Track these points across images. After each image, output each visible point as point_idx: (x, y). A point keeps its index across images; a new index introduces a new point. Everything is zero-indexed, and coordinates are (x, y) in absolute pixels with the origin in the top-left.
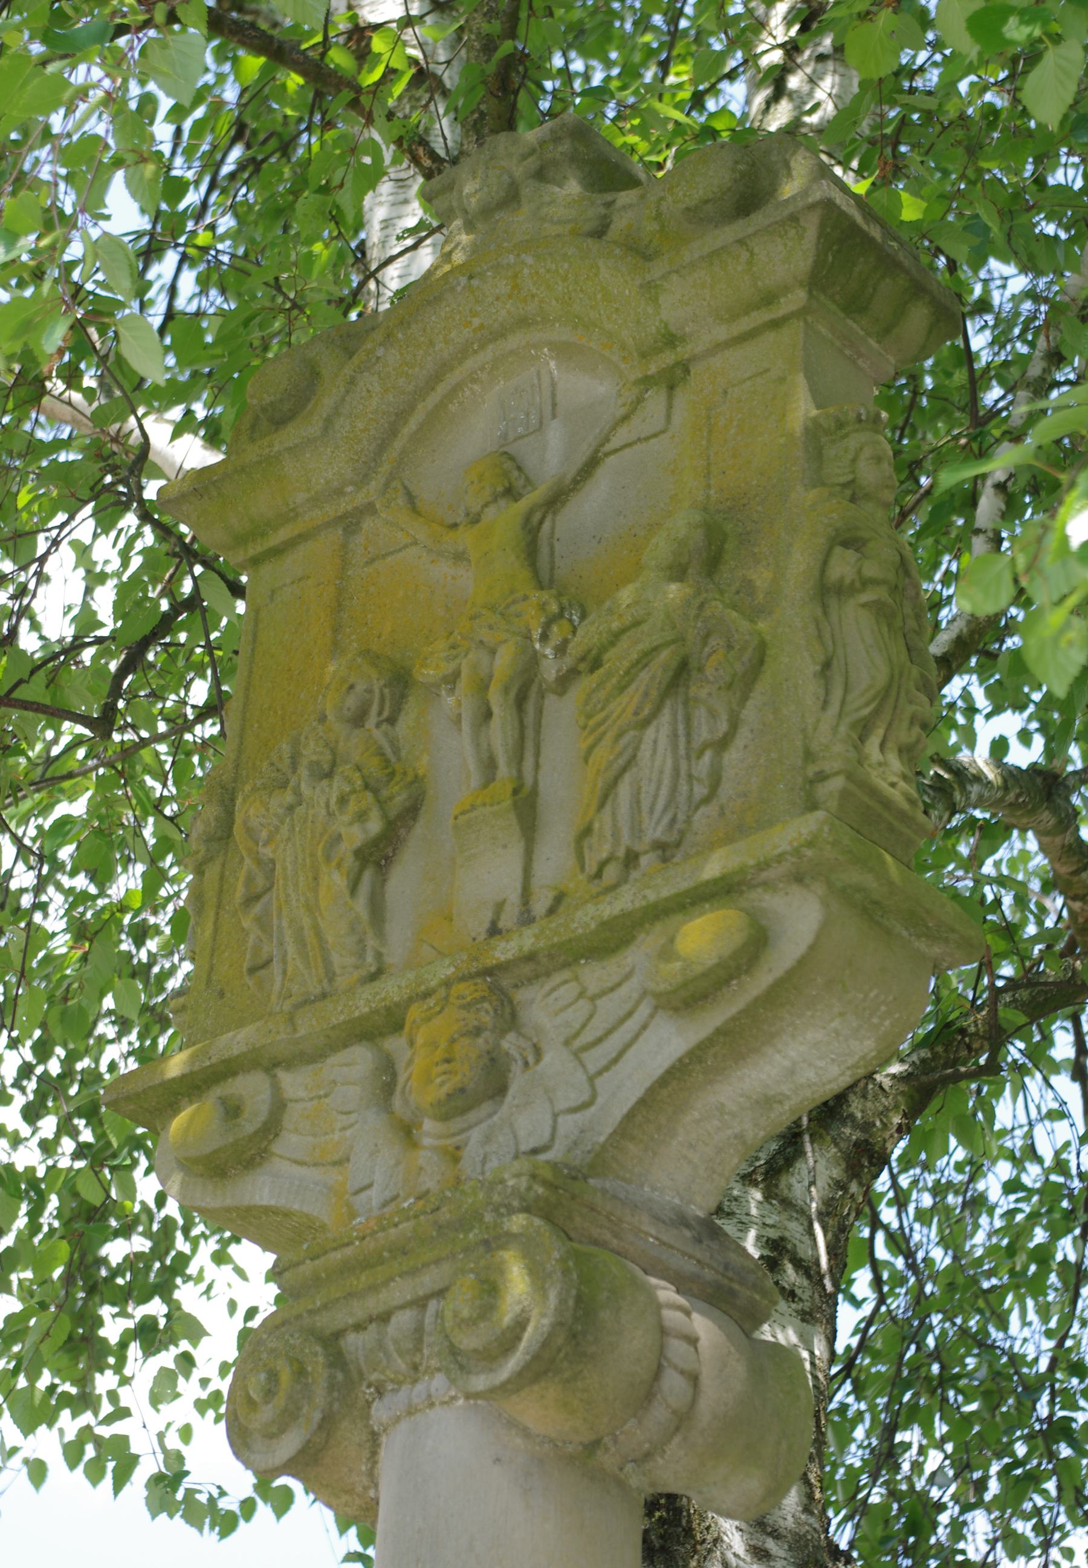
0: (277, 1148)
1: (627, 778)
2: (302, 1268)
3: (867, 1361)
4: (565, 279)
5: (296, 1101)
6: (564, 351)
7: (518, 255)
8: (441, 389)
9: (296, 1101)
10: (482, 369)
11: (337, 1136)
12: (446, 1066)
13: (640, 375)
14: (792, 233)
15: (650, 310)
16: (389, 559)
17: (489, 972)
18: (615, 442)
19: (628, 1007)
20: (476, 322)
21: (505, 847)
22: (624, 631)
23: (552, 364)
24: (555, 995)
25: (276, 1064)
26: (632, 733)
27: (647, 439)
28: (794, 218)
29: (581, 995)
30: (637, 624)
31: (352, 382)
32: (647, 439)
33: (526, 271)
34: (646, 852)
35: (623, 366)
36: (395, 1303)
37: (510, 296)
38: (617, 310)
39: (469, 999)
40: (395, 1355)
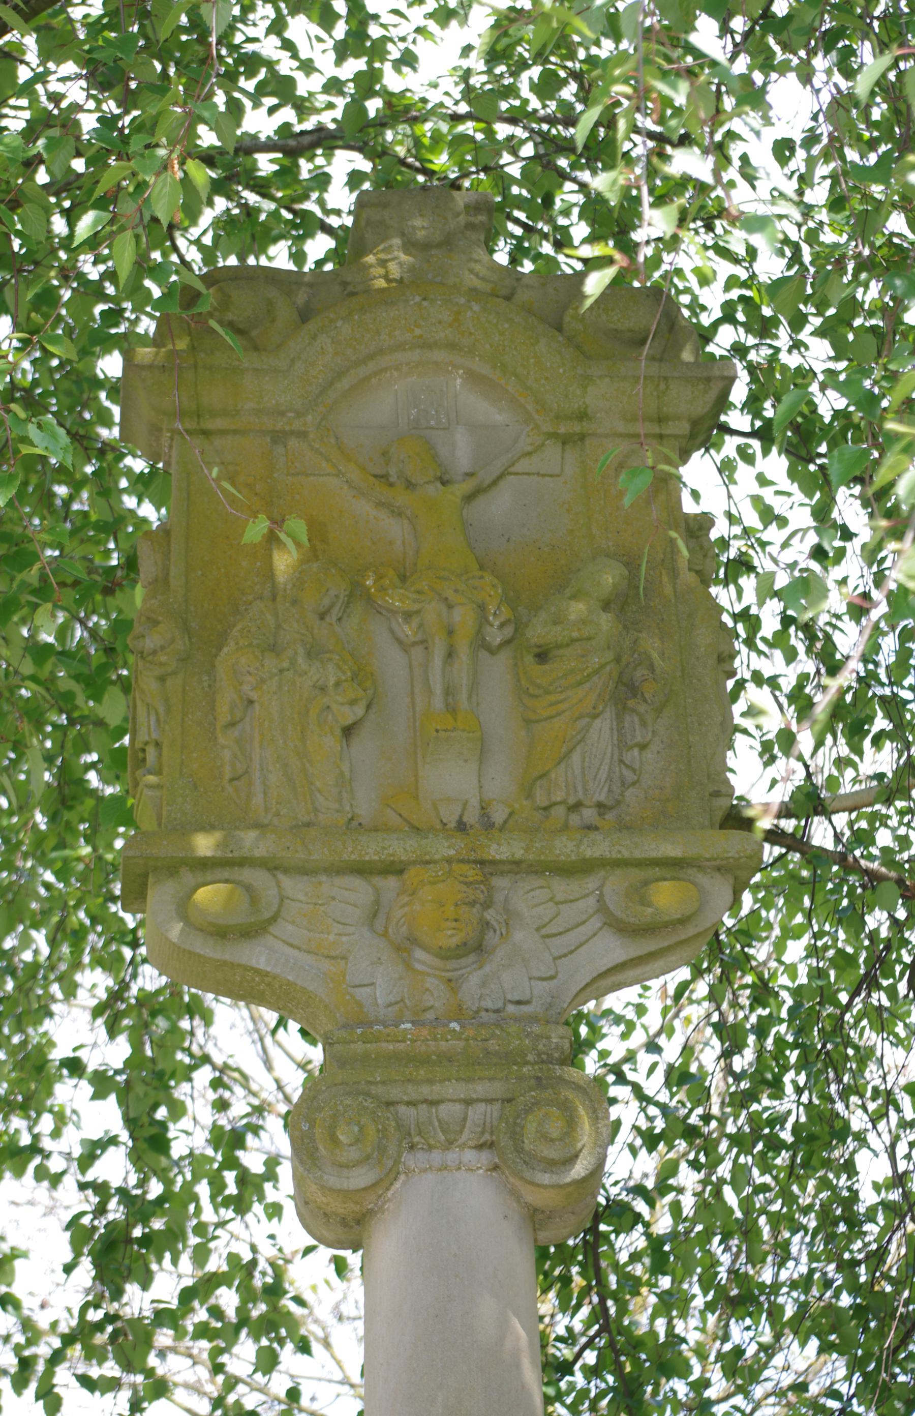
0: (273, 929)
1: (578, 748)
2: (353, 1046)
3: (34, 905)
4: (502, 334)
5: (293, 900)
6: (472, 378)
7: (469, 301)
8: (372, 366)
9: (293, 900)
10: (408, 364)
11: (332, 938)
12: (454, 924)
13: (551, 430)
14: (701, 387)
15: (578, 392)
16: (312, 478)
17: (482, 863)
18: (517, 468)
19: (584, 917)
20: (418, 332)
21: (466, 761)
22: (577, 640)
23: (459, 381)
24: (532, 894)
25: (276, 868)
26: (587, 720)
27: (544, 475)
28: (709, 380)
29: (551, 899)
30: (589, 639)
31: (314, 337)
32: (544, 475)
33: (469, 314)
34: (590, 807)
35: (537, 417)
36: (449, 1097)
37: (451, 325)
38: (547, 378)
39: (471, 879)
40: (439, 1130)
